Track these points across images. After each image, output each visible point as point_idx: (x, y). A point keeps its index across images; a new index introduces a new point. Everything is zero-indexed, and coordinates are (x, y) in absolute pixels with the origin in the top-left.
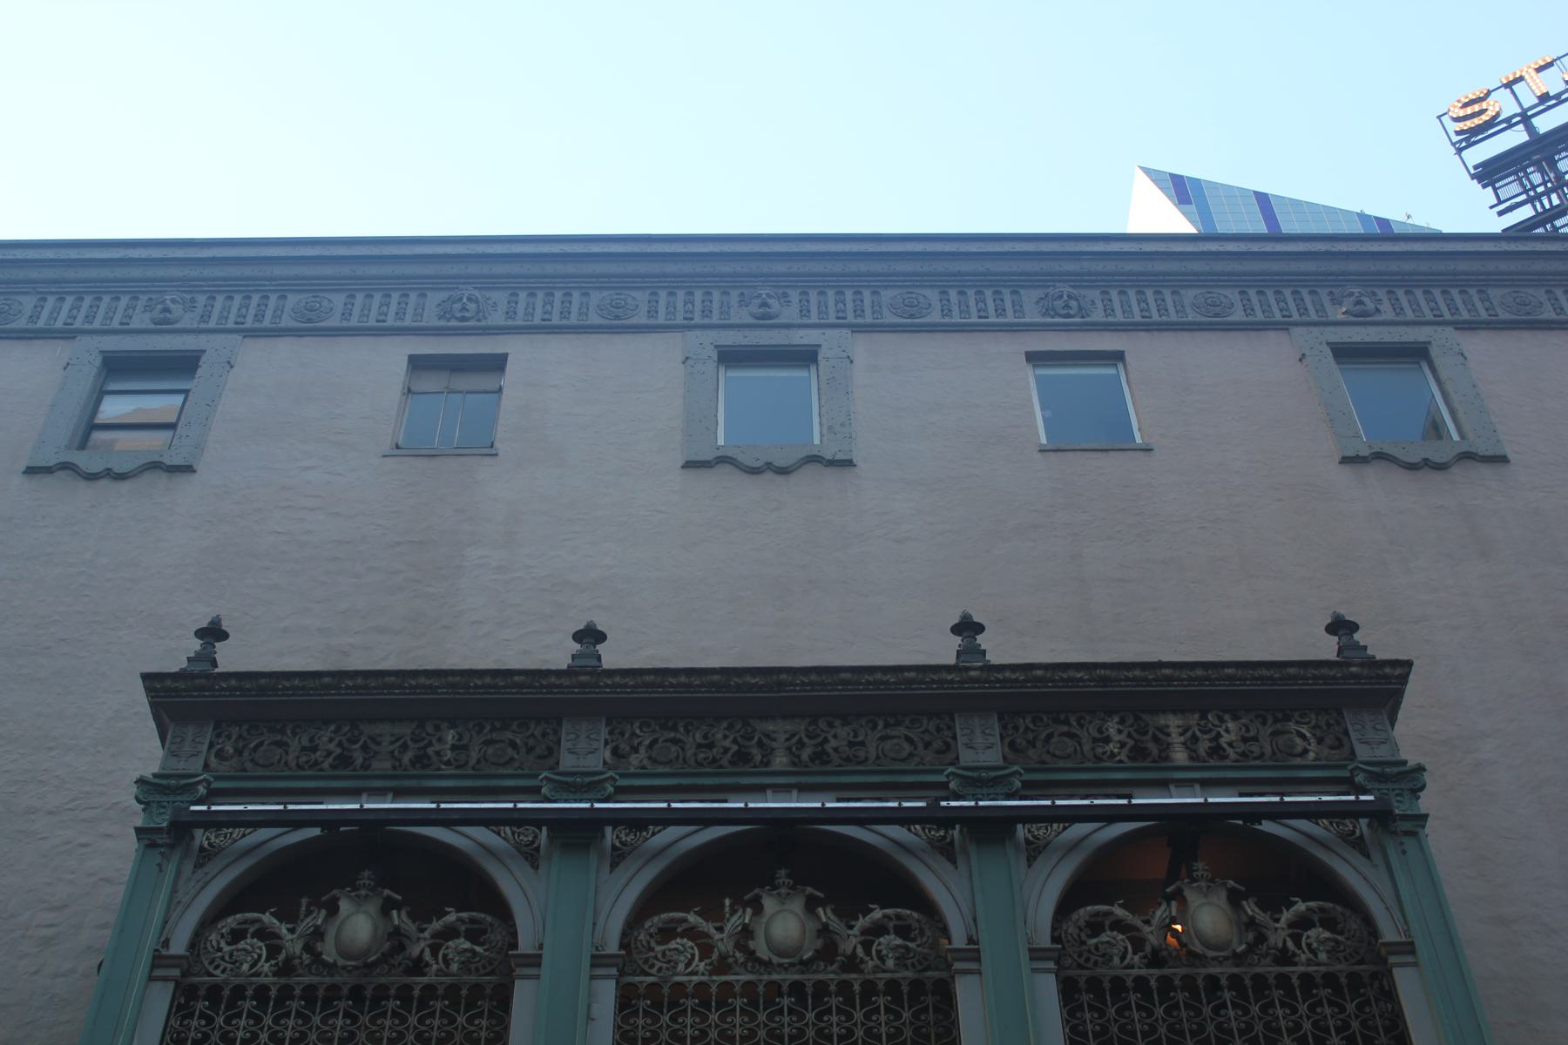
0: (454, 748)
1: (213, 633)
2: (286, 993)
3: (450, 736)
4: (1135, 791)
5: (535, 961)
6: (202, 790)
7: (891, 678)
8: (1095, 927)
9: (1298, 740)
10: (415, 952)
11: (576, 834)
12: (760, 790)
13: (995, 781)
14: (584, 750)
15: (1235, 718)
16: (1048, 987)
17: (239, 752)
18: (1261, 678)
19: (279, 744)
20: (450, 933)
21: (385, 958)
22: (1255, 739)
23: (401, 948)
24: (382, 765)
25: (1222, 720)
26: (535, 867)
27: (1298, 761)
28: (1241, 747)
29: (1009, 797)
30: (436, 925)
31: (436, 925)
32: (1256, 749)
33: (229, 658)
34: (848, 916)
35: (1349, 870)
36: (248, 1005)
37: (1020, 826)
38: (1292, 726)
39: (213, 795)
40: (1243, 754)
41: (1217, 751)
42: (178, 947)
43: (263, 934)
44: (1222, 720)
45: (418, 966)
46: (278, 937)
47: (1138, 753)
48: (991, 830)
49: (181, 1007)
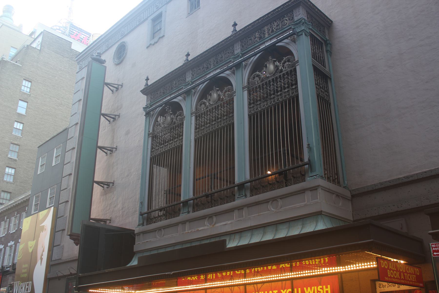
0: (277, 26)
1: (235, 25)
2: (263, 84)
3: (276, 24)
4: (260, 46)
5: (298, 62)
6: (241, 55)
7: (232, 37)
8: (254, 78)
9: (286, 21)
10: (280, 68)
11: (238, 66)
12: (210, 73)
13: (238, 56)
14: (238, 50)
15: (276, 22)
16: (246, 93)
17: (245, 44)
18: (277, 12)
19: (251, 39)
20: (226, 91)
21: (276, 72)
22: (279, 25)
23: (278, 69)
24: (267, 36)
25: (273, 23)
26: (234, 74)
27: (285, 26)
28: (276, 28)
29: (241, 58)
30: (282, 62)
31: (282, 62)
32: (278, 27)
33: (238, 28)
34: (279, 62)
35: (292, 48)
36: (286, 76)
37: (243, 63)
38: (285, 18)
39: (243, 55)
40: (277, 30)
41: (273, 31)
42: (246, 84)
43: (258, 76)
44: (273, 23)
45: (281, 71)
46: (260, 75)
47: (260, 38)
48: (238, 66)
49: (249, 94)
